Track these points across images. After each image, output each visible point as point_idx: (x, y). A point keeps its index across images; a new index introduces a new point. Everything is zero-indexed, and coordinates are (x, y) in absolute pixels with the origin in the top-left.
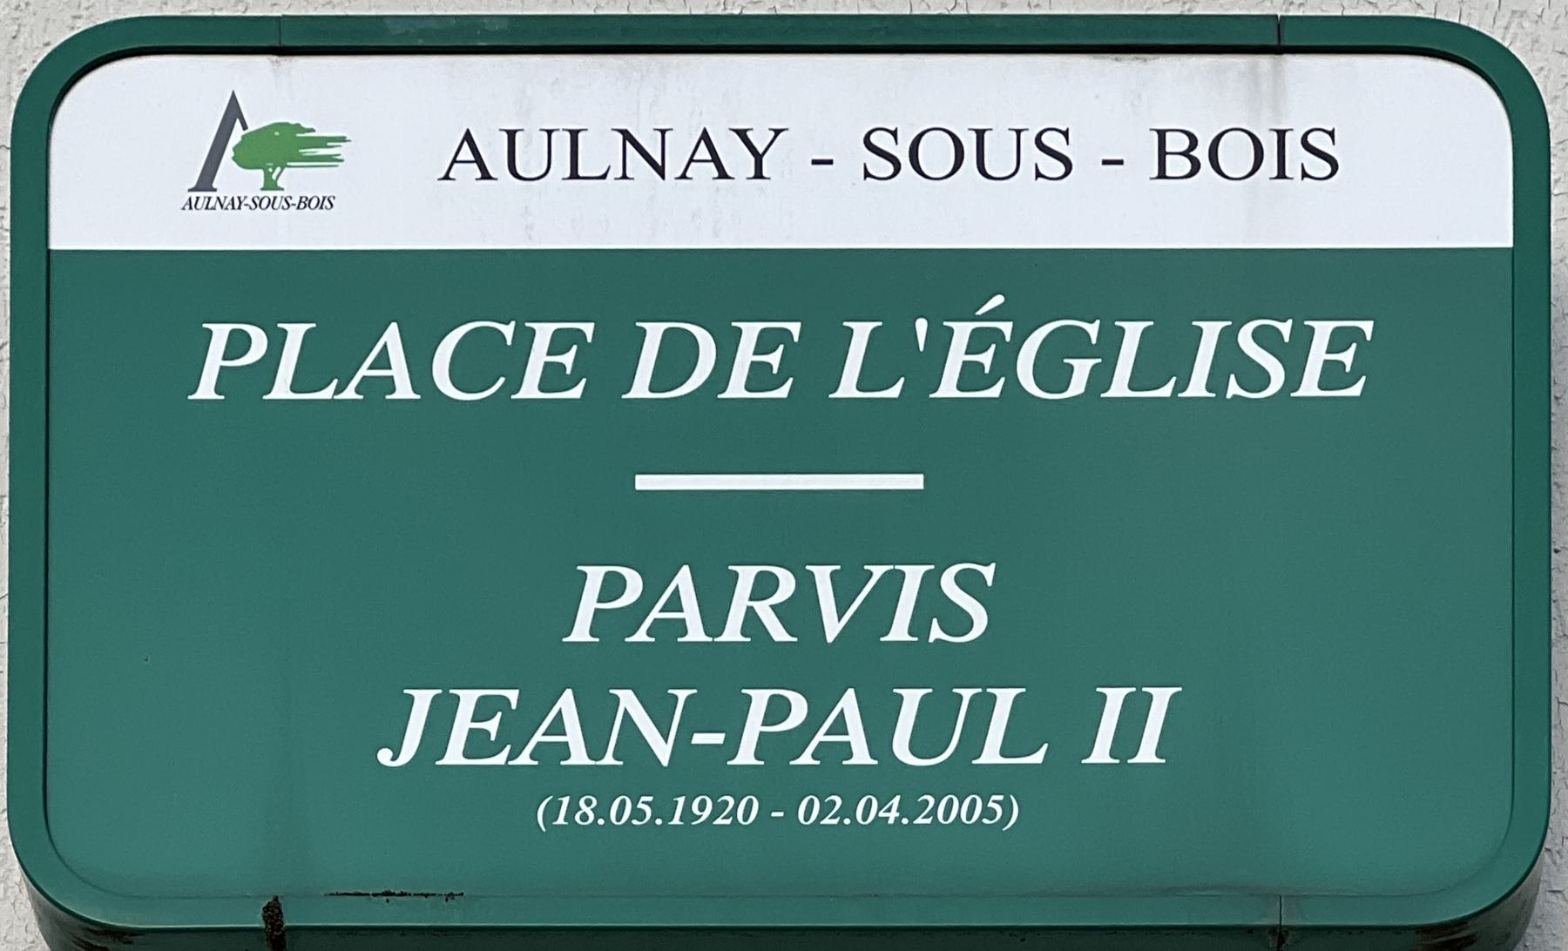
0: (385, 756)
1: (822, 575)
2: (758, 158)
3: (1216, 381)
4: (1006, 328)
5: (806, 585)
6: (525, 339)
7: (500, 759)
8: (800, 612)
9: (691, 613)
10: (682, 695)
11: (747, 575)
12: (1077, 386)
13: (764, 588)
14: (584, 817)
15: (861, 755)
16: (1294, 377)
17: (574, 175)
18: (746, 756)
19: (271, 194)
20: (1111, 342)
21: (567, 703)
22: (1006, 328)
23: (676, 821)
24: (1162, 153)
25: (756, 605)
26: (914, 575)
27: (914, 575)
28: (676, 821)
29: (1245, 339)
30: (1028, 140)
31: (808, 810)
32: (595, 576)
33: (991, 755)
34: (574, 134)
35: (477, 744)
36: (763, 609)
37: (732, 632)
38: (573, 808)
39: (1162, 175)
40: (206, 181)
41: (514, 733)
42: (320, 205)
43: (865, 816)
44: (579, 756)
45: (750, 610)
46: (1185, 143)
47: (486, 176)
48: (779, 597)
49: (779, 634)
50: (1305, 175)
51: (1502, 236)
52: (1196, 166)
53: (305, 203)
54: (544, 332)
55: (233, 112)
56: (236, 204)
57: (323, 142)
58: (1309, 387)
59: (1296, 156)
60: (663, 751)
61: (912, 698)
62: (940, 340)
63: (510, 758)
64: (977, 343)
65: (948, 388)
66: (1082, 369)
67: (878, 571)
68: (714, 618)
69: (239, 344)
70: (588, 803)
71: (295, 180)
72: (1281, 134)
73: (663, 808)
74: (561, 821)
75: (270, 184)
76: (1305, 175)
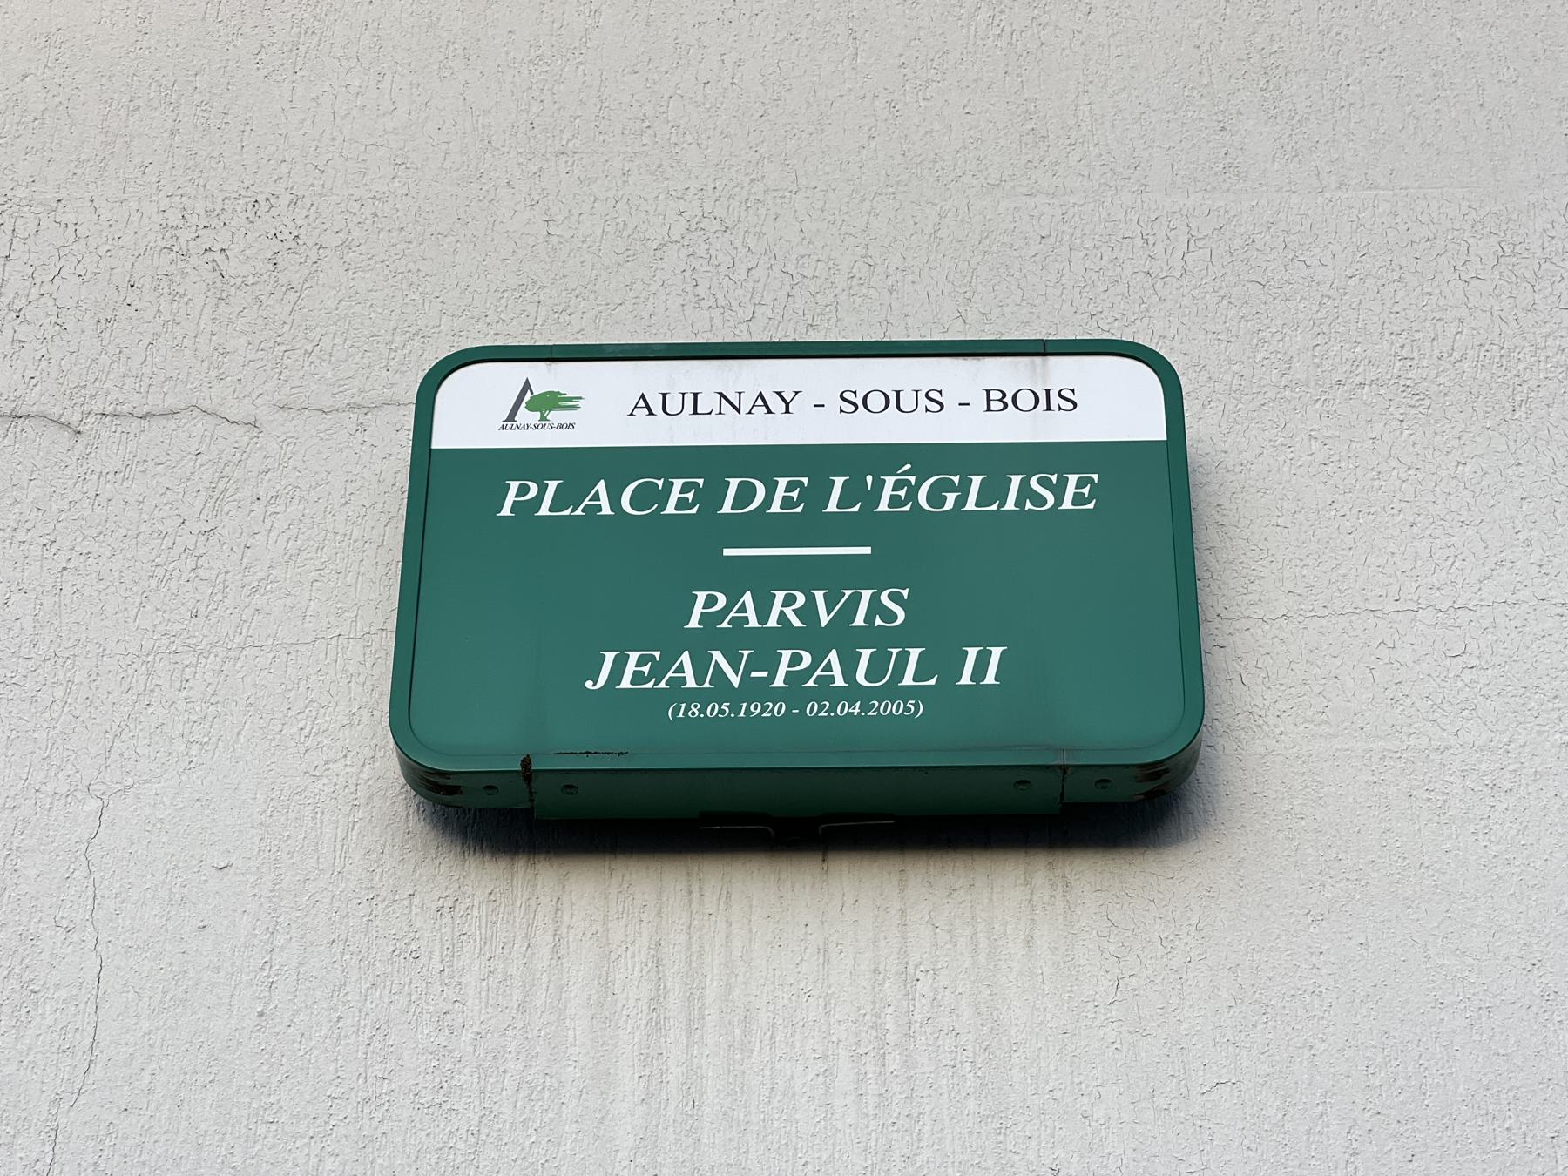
0: (589, 684)
1: (819, 595)
2: (787, 404)
3: (1020, 502)
4: (912, 479)
5: (811, 600)
6: (669, 487)
7: (650, 685)
8: (808, 612)
10: (746, 653)
11: (780, 595)
12: (949, 505)
13: (789, 601)
14: (693, 713)
15: (840, 681)
16: (1059, 499)
17: (695, 412)
18: (779, 682)
19: (543, 423)
20: (964, 488)
21: (685, 658)
22: (912, 479)
23: (742, 715)
24: (989, 400)
25: (785, 609)
26: (866, 595)
27: (866, 595)
28: (742, 715)
29: (1034, 483)
30: (922, 395)
31: (812, 709)
32: (701, 597)
33: (908, 680)
34: (696, 395)
35: (638, 678)
36: (789, 611)
37: (772, 622)
38: (688, 709)
39: (989, 409)
40: (511, 417)
41: (658, 673)
42: (568, 427)
43: (842, 711)
44: (691, 683)
45: (782, 612)
46: (1000, 395)
47: (651, 413)
48: (796, 606)
49: (796, 623)
50: (1060, 409)
51: (1162, 436)
52: (1006, 406)
53: (560, 426)
54: (678, 483)
55: (527, 386)
56: (527, 427)
57: (571, 399)
58: (1067, 504)
60: (735, 680)
61: (866, 654)
62: (879, 486)
63: (655, 684)
65: (883, 507)
66: (951, 498)
67: (848, 593)
68: (763, 615)
69: (523, 490)
70: (695, 706)
71: (555, 416)
72: (1048, 391)
73: (735, 709)
74: (681, 715)
75: (543, 418)
76: (1060, 409)
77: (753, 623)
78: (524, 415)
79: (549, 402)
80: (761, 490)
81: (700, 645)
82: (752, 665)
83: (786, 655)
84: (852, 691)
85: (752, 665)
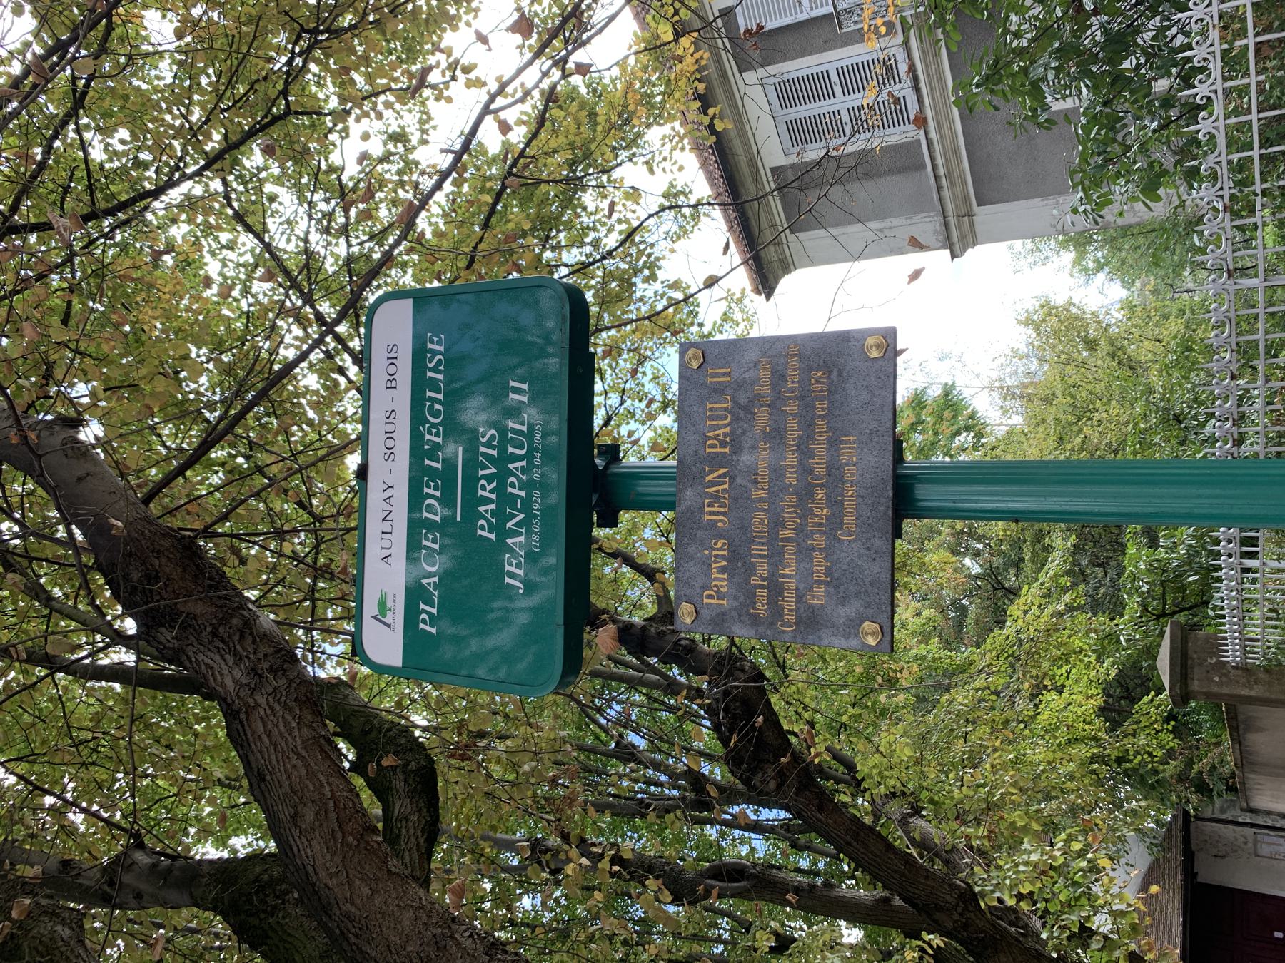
1: (481, 473)
3: (439, 372)
5: (484, 477)
8: (489, 478)
9: (489, 507)
12: (440, 407)
13: (483, 488)
15: (524, 463)
18: (523, 494)
20: (431, 399)
26: (482, 449)
27: (482, 449)
29: (431, 365)
32: (480, 532)
36: (489, 488)
37: (494, 496)
40: (389, 626)
49: (494, 484)
51: (411, 301)
54: (424, 543)
55: (374, 617)
58: (442, 349)
59: (392, 355)
60: (521, 516)
61: (511, 450)
64: (430, 433)
66: (437, 406)
68: (490, 501)
69: (424, 621)
71: (389, 604)
73: (535, 516)
77: (493, 506)
78: (388, 620)
79: (382, 605)
80: (429, 501)
81: (503, 533)
82: (514, 507)
83: (510, 490)
84: (529, 456)
85: (514, 507)
